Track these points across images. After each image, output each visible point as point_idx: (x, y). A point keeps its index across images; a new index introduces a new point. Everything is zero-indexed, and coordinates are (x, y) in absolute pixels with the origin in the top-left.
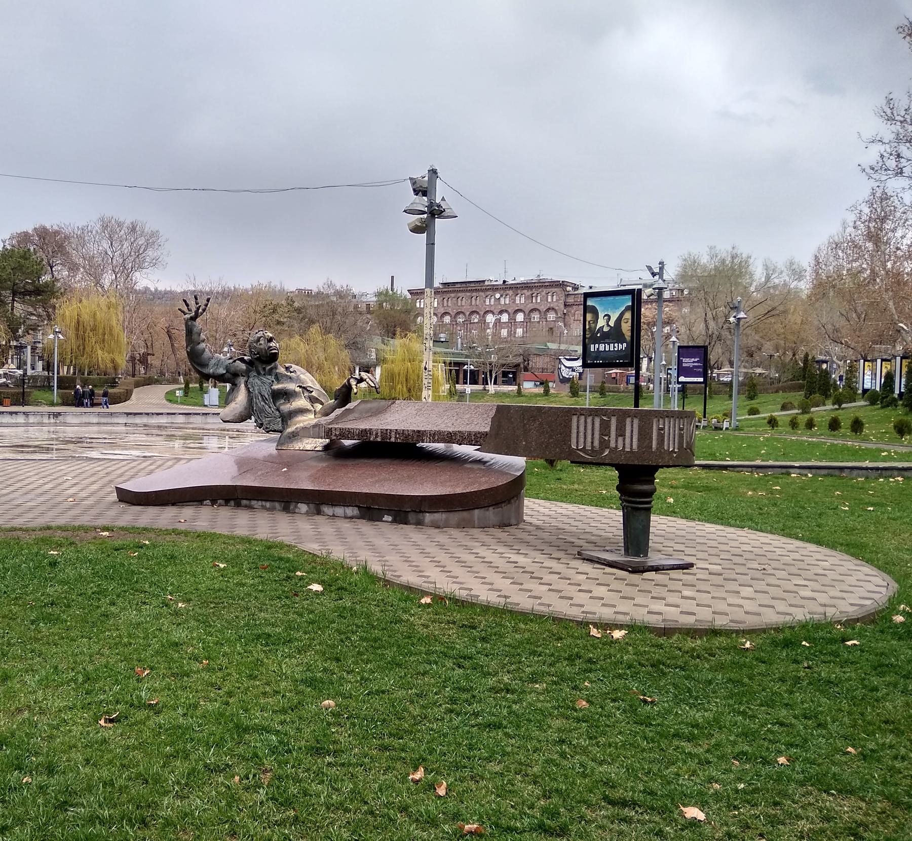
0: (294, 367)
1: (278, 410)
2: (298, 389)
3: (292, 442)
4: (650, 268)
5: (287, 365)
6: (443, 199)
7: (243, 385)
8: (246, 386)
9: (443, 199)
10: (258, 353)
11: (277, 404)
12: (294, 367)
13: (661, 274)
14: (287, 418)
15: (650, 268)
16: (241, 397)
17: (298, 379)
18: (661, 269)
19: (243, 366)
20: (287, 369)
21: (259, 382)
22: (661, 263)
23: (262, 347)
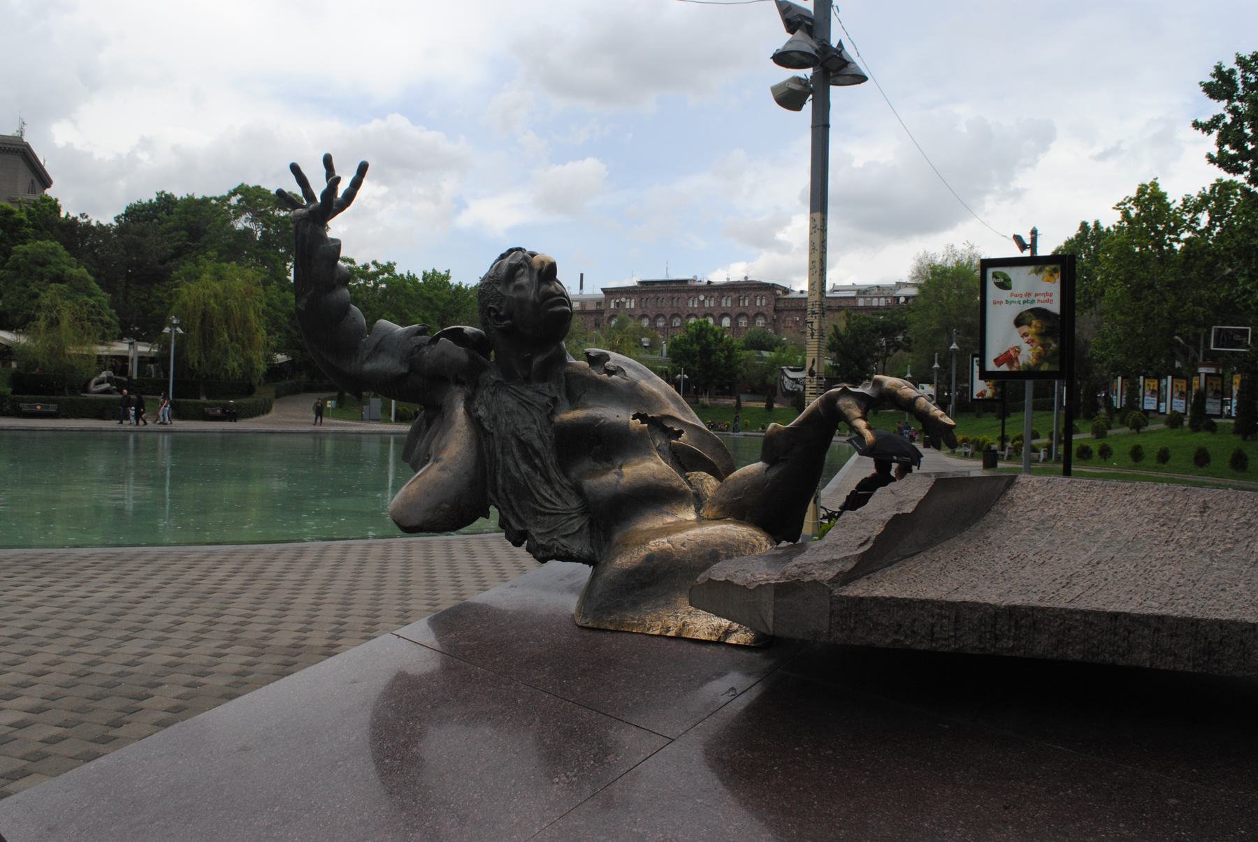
0: (615, 358)
1: (578, 490)
2: (636, 424)
3: (635, 605)
4: (1018, 239)
5: (594, 350)
6: (840, 44)
7: (460, 410)
8: (469, 411)
9: (840, 44)
10: (510, 315)
11: (573, 474)
12: (615, 358)
13: (1033, 246)
14: (612, 515)
15: (1018, 239)
16: (455, 445)
17: (632, 395)
18: (1034, 240)
19: (460, 353)
20: (597, 361)
21: (511, 404)
22: (1034, 233)
23: (521, 294)
